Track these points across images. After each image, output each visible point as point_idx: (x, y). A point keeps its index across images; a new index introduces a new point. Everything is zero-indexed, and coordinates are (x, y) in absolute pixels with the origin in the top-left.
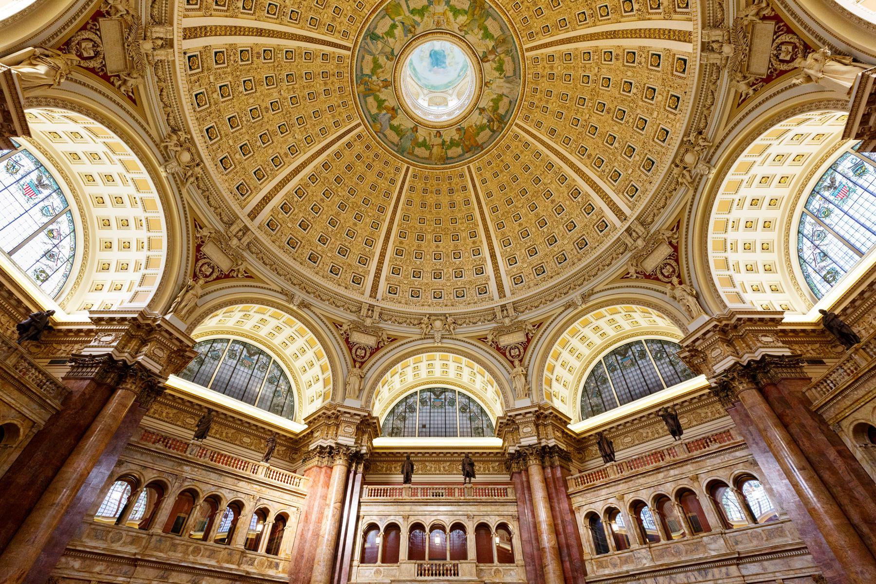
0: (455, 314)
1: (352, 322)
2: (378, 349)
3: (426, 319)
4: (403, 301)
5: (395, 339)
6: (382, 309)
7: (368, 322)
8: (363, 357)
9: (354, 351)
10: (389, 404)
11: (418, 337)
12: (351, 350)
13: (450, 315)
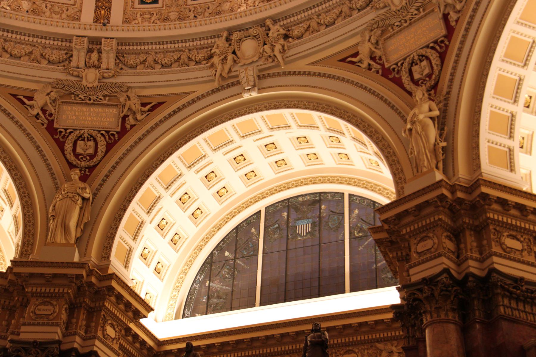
0: (285, 16)
1: (56, 85)
2: (123, 132)
3: (221, 42)
4: (173, 15)
5: (160, 104)
6: (121, 42)
7: (91, 77)
8: (92, 157)
9: (68, 147)
10: (199, 248)
11: (209, 87)
12: (61, 146)
13: (275, 20)
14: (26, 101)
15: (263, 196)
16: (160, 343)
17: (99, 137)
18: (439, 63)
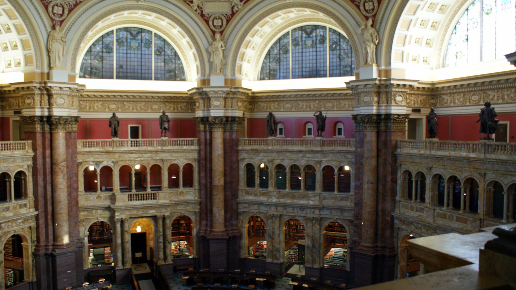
2: (233, 14)
8: (221, 27)
9: (211, 23)
12: (207, 22)
14: (190, 4)
15: (290, 25)
16: (253, 93)
17: (223, 18)
18: (377, 6)
